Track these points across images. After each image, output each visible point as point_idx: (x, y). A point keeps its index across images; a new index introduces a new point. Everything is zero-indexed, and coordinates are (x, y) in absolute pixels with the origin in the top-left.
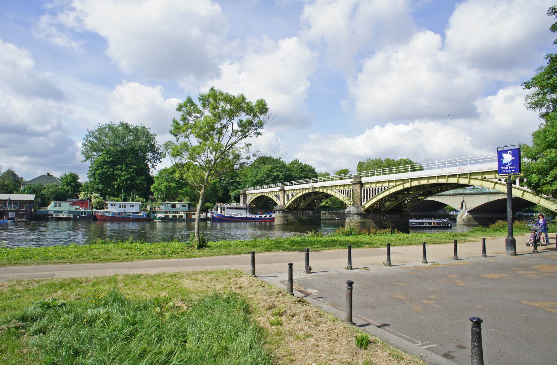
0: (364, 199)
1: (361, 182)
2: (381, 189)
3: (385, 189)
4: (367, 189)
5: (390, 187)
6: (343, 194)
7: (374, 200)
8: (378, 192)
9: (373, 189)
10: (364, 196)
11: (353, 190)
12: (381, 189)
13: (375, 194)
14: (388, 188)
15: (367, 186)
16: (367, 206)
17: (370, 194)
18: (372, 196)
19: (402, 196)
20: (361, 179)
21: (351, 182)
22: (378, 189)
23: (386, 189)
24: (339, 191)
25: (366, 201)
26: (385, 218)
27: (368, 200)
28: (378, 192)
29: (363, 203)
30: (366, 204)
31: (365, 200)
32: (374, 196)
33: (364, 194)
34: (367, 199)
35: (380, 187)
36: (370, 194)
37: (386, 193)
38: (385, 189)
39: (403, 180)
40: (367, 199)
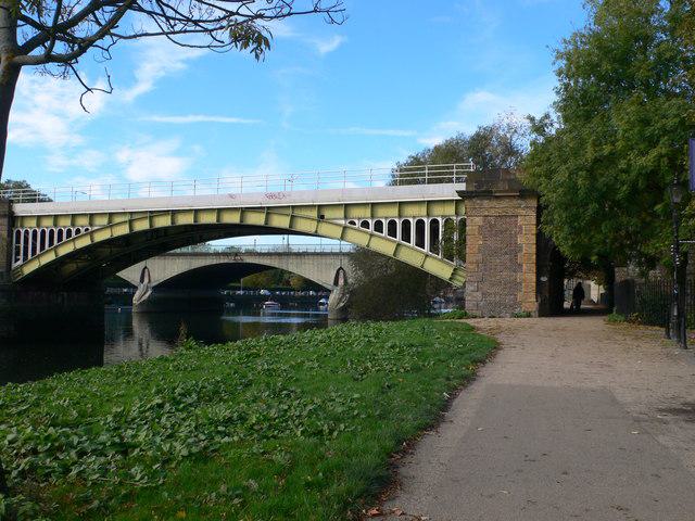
0: (18, 253)
2: (69, 232)
3: (78, 231)
4: (27, 232)
7: (49, 258)
8: (60, 239)
9: (43, 232)
10: (18, 248)
12: (69, 232)
13: (51, 243)
14: (87, 230)
16: (28, 269)
20: (10, 207)
22: (60, 232)
23: (82, 230)
26: (60, 300)
28: (60, 239)
29: (14, 265)
31: (21, 257)
33: (18, 241)
35: (65, 227)
37: (84, 242)
38: (78, 231)
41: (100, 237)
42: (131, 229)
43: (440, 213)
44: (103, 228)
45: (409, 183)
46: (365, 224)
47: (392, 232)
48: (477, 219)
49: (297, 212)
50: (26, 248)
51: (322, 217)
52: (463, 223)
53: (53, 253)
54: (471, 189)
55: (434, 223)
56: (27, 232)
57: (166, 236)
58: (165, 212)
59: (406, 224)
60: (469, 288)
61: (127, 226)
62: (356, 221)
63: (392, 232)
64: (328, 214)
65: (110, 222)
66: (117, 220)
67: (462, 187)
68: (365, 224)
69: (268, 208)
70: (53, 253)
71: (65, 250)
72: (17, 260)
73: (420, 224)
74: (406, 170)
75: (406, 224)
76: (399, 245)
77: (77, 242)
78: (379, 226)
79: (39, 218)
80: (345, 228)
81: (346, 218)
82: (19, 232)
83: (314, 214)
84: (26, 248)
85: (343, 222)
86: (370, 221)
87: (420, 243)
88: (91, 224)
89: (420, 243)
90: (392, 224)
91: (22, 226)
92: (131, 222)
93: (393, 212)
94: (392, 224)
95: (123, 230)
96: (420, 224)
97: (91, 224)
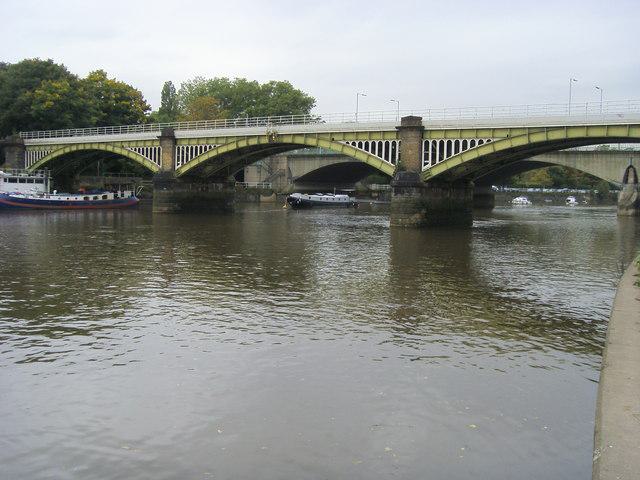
0: (178, 160)
2: (206, 148)
3: (210, 147)
7: (194, 163)
8: (201, 152)
12: (206, 148)
16: (184, 170)
28: (201, 152)
34: (183, 161)
37: (213, 154)
38: (210, 147)
40: (183, 161)
44: (224, 145)
47: (367, 148)
59: (374, 144)
68: (354, 144)
78: (360, 145)
90: (367, 144)
94: (367, 144)
95: (232, 147)
96: (380, 144)
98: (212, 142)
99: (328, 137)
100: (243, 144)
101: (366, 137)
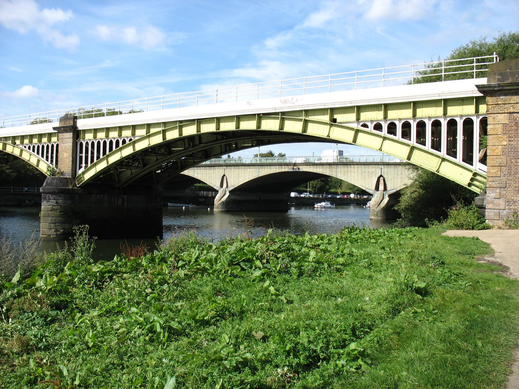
0: (81, 163)
1: (77, 127)
2: (117, 142)
3: (124, 142)
4: (87, 143)
5: (137, 138)
6: (38, 153)
7: (102, 165)
8: (111, 149)
9: (99, 143)
10: (81, 158)
11: (57, 145)
12: (118, 142)
14: (131, 140)
15: (89, 136)
16: (88, 176)
17: (92, 153)
18: (98, 158)
19: (155, 158)
20: (75, 123)
21: (54, 128)
22: (111, 142)
23: (128, 142)
24: (29, 148)
25: (86, 167)
26: (120, 202)
27: (89, 165)
28: (111, 149)
30: (83, 173)
31: (84, 165)
32: (101, 157)
33: (81, 152)
34: (86, 163)
36: (92, 153)
37: (128, 151)
38: (124, 142)
39: (165, 124)
40: (86, 163)
41: (141, 146)
42: (164, 137)
43: (423, 113)
44: (142, 138)
45: (427, 81)
46: (378, 127)
47: (406, 134)
48: (500, 117)
49: (311, 118)
50: (87, 158)
51: (335, 120)
52: (484, 123)
53: (105, 162)
54: (493, 83)
55: (452, 124)
56: (87, 143)
57: (200, 143)
58: (191, 122)
59: (421, 125)
60: (491, 195)
61: (161, 135)
62: (369, 124)
63: (406, 134)
64: (339, 117)
65: (148, 131)
66: (153, 131)
67: (57, 124)
68: (378, 127)
69: (283, 113)
70: (105, 162)
71: (114, 158)
72: (80, 167)
73: (436, 124)
74: (451, 63)
75: (421, 125)
76: (413, 148)
77: (123, 151)
78: (392, 129)
79: (121, 129)
80: (357, 131)
81: (358, 119)
82: (81, 144)
83: (326, 118)
84: (87, 158)
85: (355, 126)
86: (383, 123)
87: (436, 146)
88: (133, 134)
89: (436, 146)
90: (406, 126)
91: (84, 138)
92: (164, 132)
93: (406, 114)
94: (406, 126)
95: (158, 140)
96: (436, 124)
97: (133, 134)
98: (127, 133)
99: (326, 118)
100: (172, 135)
101: (406, 114)
